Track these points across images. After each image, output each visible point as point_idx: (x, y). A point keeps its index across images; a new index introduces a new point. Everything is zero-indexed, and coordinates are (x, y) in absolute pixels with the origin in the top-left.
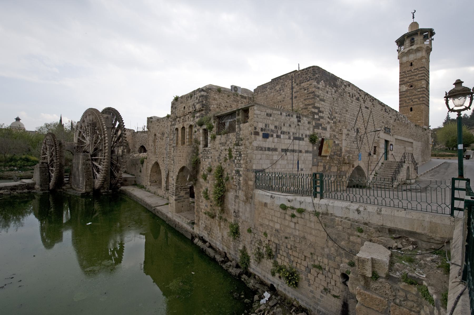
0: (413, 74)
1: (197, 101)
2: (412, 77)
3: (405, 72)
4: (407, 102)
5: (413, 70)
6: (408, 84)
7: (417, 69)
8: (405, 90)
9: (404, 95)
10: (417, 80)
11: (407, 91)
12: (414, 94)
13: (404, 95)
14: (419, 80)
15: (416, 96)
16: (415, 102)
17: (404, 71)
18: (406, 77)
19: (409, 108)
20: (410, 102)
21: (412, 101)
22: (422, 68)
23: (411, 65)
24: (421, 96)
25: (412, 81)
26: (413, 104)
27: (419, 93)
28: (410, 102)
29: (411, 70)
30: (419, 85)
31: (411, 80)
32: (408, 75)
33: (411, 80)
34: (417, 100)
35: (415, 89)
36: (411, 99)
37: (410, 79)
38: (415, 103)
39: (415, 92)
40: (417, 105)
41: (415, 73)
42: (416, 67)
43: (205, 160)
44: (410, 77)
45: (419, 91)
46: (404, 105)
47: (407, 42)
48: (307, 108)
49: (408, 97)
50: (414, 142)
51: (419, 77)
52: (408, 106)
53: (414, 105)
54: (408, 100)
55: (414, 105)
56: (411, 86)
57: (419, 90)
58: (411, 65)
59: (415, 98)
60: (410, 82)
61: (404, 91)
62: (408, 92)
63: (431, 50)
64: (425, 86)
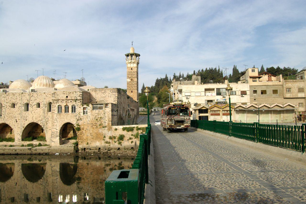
1: (78, 96)
2: (132, 75)
3: (129, 72)
4: (130, 87)
6: (131, 78)
7: (134, 72)
8: (129, 81)
9: (129, 84)
10: (134, 78)
11: (130, 82)
12: (132, 84)
13: (129, 84)
14: (134, 78)
15: (134, 85)
17: (129, 71)
18: (130, 75)
19: (131, 91)
20: (131, 88)
22: (136, 72)
23: (132, 69)
24: (135, 85)
26: (132, 89)
27: (135, 84)
28: (131, 88)
29: (131, 72)
30: (135, 80)
31: (131, 77)
32: (130, 74)
33: (131, 77)
34: (134, 87)
35: (134, 82)
36: (132, 86)
37: (131, 76)
38: (133, 89)
39: (133, 83)
40: (134, 90)
41: (133, 74)
43: (85, 119)
44: (131, 75)
45: (135, 83)
46: (129, 89)
47: (130, 57)
48: (115, 101)
49: (131, 85)
50: (135, 109)
53: (133, 90)
55: (133, 90)
56: (132, 80)
57: (135, 82)
58: (132, 69)
60: (131, 78)
61: (129, 82)
62: (131, 83)
63: (139, 63)
64: (136, 81)
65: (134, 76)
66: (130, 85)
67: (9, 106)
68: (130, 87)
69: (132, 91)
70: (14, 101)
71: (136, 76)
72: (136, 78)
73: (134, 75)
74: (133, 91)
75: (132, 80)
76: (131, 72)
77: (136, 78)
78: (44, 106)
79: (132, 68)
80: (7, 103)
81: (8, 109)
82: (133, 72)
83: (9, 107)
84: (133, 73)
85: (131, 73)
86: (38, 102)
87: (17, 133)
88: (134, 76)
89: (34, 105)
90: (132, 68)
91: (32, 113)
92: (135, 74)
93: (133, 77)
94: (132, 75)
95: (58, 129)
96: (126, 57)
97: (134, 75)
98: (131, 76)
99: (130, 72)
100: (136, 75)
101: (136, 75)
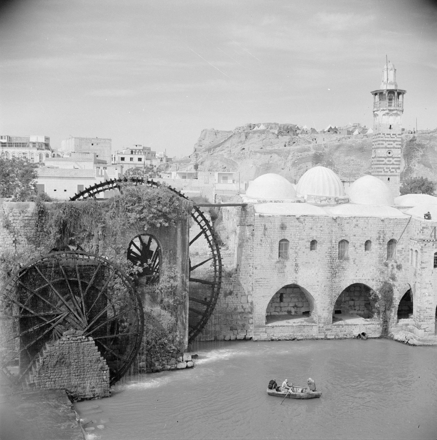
0: (392, 139)
5: (391, 135)
6: (387, 150)
7: (395, 134)
12: (391, 163)
14: (396, 148)
16: (392, 172)
21: (390, 170)
22: (399, 135)
25: (391, 148)
26: (390, 174)
28: (387, 172)
29: (390, 134)
32: (387, 139)
33: (388, 146)
34: (394, 170)
37: (389, 144)
38: (393, 174)
41: (394, 139)
42: (394, 133)
46: (383, 173)
51: (397, 145)
52: (386, 176)
54: (387, 168)
57: (396, 159)
58: (390, 128)
59: (392, 168)
60: (389, 148)
65: (394, 145)
66: (384, 164)
67: (304, 247)
68: (384, 170)
69: (389, 179)
70: (314, 235)
71: (400, 145)
72: (398, 148)
73: (394, 141)
74: (390, 178)
75: (389, 153)
76: (390, 134)
77: (398, 148)
78: (381, 249)
79: (391, 126)
80: (299, 239)
81: (304, 252)
82: (393, 135)
83: (306, 248)
84: (394, 136)
85: (388, 138)
86: (369, 239)
87: (322, 307)
88: (394, 145)
89: (360, 246)
90: (391, 126)
91: (357, 263)
92: (398, 139)
93: (392, 146)
94: (390, 141)
95: (433, 303)
96: (373, 96)
97: (394, 141)
98: (389, 144)
99: (387, 134)
100: (399, 141)
101: (399, 141)
